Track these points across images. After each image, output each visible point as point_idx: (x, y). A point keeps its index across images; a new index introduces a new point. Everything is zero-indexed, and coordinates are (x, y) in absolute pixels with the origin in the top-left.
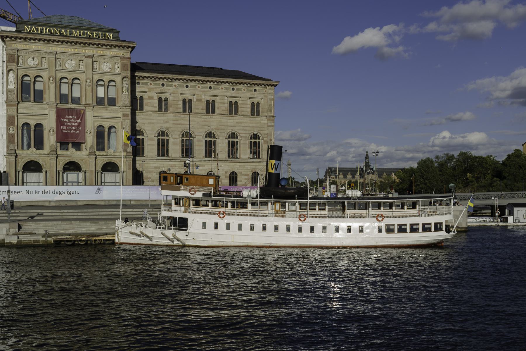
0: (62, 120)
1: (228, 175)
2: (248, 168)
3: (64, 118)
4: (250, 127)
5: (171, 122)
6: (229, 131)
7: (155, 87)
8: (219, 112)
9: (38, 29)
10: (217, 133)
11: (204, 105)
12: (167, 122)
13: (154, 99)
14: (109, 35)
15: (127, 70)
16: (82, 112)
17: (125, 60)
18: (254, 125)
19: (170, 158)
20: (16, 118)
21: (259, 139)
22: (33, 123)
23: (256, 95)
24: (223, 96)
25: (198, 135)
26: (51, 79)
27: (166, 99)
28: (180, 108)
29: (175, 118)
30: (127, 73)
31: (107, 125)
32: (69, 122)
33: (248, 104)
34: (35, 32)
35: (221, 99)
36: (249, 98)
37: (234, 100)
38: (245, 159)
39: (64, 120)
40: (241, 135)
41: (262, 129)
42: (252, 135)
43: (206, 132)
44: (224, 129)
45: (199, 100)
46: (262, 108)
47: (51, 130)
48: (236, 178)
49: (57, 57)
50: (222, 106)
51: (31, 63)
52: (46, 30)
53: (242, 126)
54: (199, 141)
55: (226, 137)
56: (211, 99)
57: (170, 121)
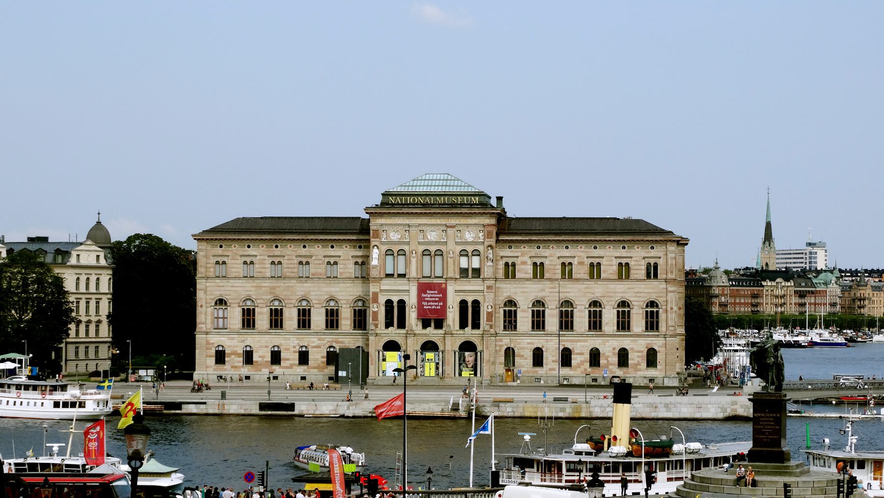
0: (423, 295)
1: (617, 351)
2: (642, 344)
3: (426, 293)
4: (644, 293)
5: (547, 290)
6: (618, 298)
7: (529, 250)
8: (605, 276)
9: (402, 199)
10: (604, 301)
11: (586, 268)
12: (543, 290)
13: (528, 265)
14: (475, 199)
15: (492, 238)
16: (444, 285)
17: (490, 227)
18: (650, 291)
19: (545, 333)
20: (379, 295)
21: (657, 306)
22: (395, 299)
23: (653, 253)
24: (611, 256)
25: (579, 305)
26: (414, 252)
27: (542, 264)
28: (557, 274)
29: (552, 286)
30: (491, 241)
31: (470, 299)
32: (431, 297)
33: (642, 265)
34: (400, 202)
35: (607, 261)
36: (644, 258)
37: (624, 261)
38: (639, 332)
39: (426, 295)
40: (633, 303)
41: (661, 295)
42: (648, 303)
43: (589, 300)
44: (612, 297)
45: (581, 263)
46: (660, 270)
47: (414, 307)
48: (627, 354)
49: (420, 228)
50: (609, 269)
51: (394, 236)
52: (410, 199)
53: (636, 293)
54: (580, 311)
55: (614, 305)
56: (595, 261)
57: (547, 290)
